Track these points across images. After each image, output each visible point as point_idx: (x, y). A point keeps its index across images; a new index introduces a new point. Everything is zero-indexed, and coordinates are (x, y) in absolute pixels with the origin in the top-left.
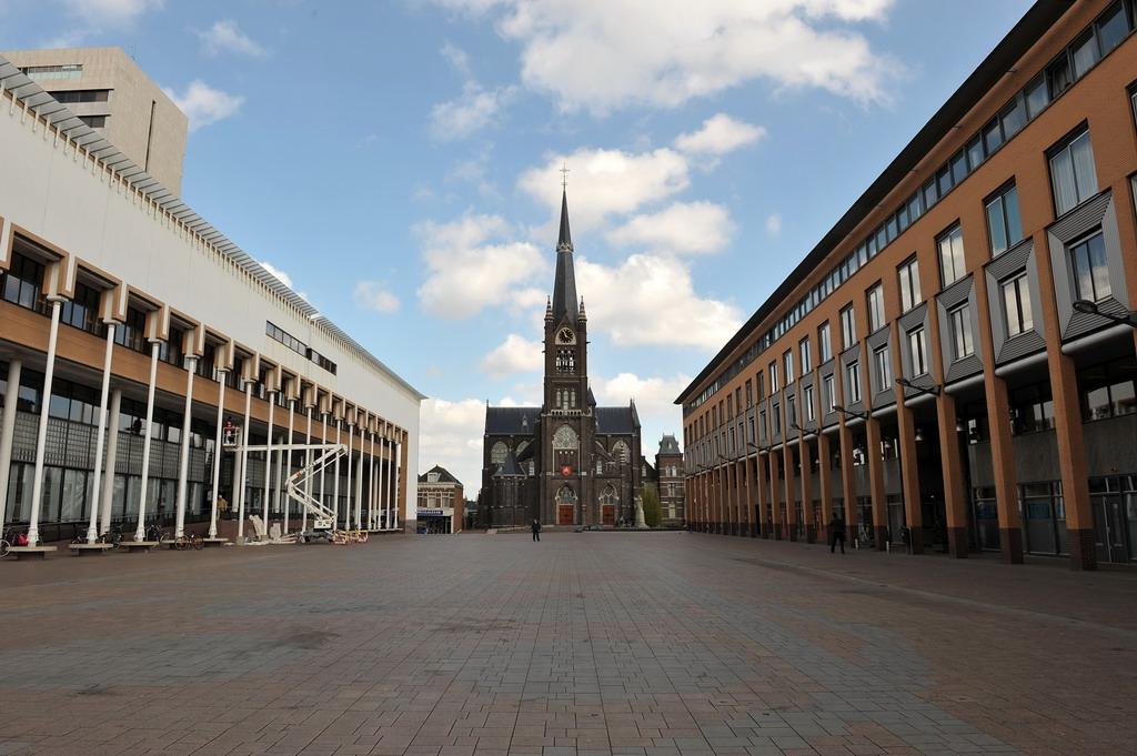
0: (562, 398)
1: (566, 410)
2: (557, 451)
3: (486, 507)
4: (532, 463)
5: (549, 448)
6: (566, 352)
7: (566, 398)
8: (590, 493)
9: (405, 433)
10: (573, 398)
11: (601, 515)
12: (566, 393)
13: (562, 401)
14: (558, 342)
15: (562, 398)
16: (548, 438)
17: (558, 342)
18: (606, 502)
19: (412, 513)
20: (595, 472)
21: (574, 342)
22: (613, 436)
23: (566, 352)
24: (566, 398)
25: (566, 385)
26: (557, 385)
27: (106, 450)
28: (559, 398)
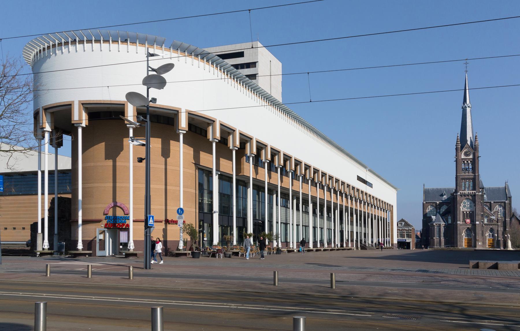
0: (465, 185)
1: (466, 192)
2: (463, 212)
3: (425, 238)
4: (449, 217)
5: (458, 210)
6: (467, 162)
7: (467, 186)
8: (480, 232)
9: (392, 206)
10: (471, 185)
11: (487, 243)
12: (467, 183)
13: (465, 187)
14: (463, 157)
15: (465, 185)
16: (458, 205)
17: (463, 157)
18: (490, 237)
19: (395, 241)
20: (483, 222)
21: (471, 157)
22: (494, 202)
23: (467, 162)
24: (467, 186)
25: (467, 179)
26: (462, 179)
27: (293, 217)
28: (463, 185)
